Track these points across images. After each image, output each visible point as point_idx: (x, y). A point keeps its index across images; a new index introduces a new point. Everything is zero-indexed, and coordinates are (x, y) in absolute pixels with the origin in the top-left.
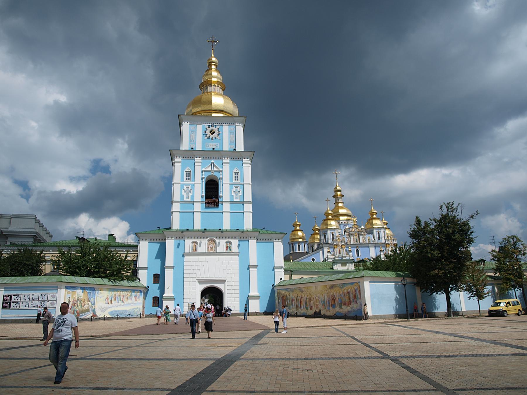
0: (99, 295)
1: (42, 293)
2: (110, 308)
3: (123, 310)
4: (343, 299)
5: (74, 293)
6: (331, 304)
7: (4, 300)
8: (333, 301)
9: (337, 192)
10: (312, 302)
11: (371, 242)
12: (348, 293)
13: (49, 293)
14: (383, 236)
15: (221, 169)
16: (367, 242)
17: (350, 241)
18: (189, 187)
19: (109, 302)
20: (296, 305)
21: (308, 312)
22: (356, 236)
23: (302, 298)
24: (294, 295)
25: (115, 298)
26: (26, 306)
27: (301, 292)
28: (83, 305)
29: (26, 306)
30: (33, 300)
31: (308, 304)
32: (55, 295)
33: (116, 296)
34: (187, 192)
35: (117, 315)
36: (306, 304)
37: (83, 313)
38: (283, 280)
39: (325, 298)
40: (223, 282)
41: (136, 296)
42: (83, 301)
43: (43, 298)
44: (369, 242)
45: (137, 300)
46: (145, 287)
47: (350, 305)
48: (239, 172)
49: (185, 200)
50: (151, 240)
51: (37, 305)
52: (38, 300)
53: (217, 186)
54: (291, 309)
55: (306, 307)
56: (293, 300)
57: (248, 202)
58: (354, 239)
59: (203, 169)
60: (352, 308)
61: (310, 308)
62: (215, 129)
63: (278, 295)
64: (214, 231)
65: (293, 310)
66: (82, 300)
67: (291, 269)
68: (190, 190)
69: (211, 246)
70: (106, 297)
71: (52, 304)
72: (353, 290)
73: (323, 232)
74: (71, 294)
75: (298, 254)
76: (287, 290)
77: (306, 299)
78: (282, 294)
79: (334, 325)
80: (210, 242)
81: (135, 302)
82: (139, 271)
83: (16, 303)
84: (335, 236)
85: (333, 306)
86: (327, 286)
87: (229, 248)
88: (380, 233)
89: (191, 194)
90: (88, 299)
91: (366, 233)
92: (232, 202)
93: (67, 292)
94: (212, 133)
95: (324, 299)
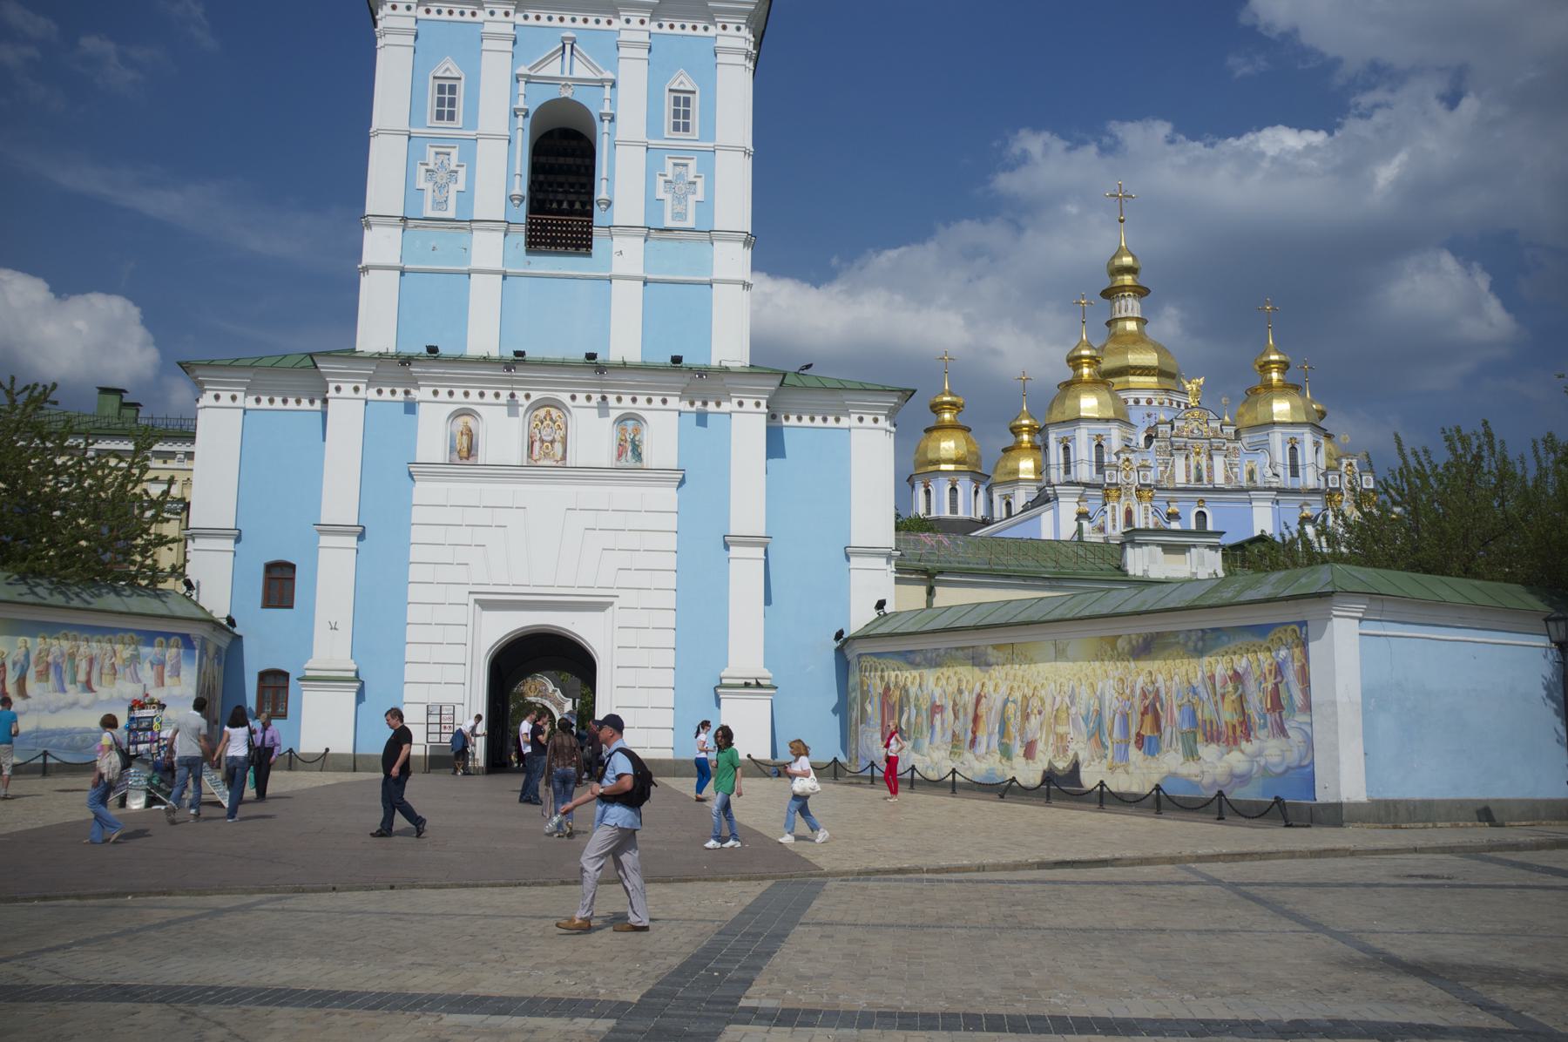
4: (1205, 712)
6: (1138, 734)
8: (1149, 718)
9: (1122, 274)
10: (1034, 721)
11: (1260, 483)
12: (1237, 677)
15: (608, 75)
16: (1245, 484)
17: (1172, 476)
18: (448, 154)
21: (1012, 768)
22: (1198, 454)
23: (983, 700)
24: (945, 683)
25: (40, 668)
31: (1013, 730)
33: (50, 659)
34: (441, 177)
35: (45, 754)
36: (1003, 730)
38: (888, 609)
39: (1107, 703)
41: (162, 664)
44: (1253, 485)
45: (167, 680)
46: (214, 624)
47: (1244, 744)
48: (694, 92)
49: (425, 215)
53: (587, 161)
54: (926, 750)
55: (1001, 744)
56: (935, 709)
57: (729, 235)
58: (1188, 467)
59: (523, 70)
60: (1252, 758)
64: (563, 365)
67: (929, 566)
68: (453, 167)
72: (1266, 667)
76: (912, 656)
79: (1200, 859)
80: (542, 413)
84: (1110, 448)
86: (1120, 641)
87: (631, 448)
88: (1297, 446)
89: (461, 186)
91: (1239, 445)
92: (655, 231)
95: (1101, 700)
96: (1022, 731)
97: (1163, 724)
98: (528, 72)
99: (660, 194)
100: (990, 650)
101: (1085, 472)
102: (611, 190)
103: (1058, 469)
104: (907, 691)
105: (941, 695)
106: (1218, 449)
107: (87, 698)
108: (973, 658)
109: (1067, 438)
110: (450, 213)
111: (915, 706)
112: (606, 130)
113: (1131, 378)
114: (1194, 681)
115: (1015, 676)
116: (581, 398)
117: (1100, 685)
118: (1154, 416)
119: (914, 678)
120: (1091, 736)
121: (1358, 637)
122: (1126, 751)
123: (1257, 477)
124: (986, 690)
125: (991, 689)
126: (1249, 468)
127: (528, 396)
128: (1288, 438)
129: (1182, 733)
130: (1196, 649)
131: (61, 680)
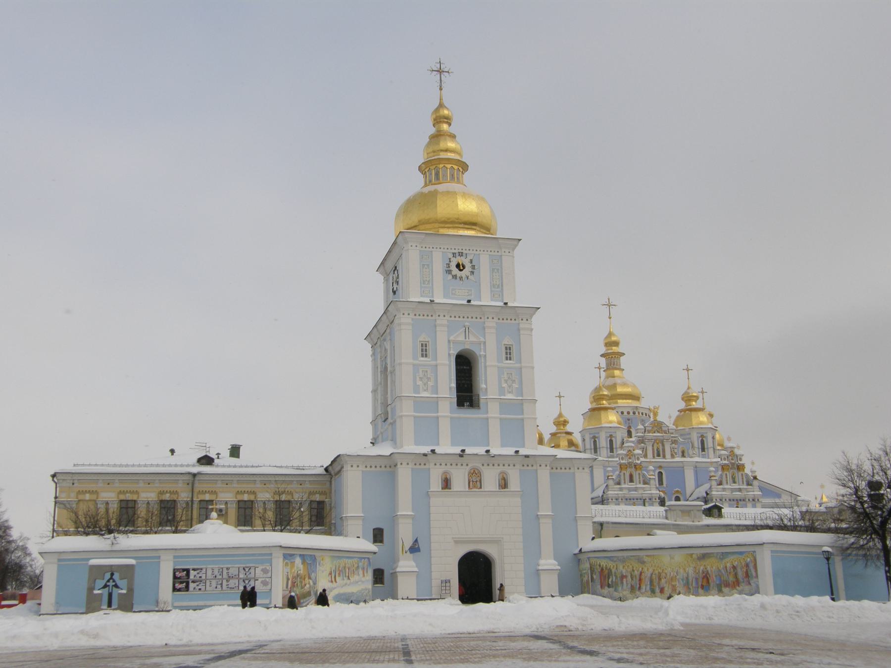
0: (321, 568)
1: (244, 566)
2: (334, 588)
3: (349, 593)
5: (293, 563)
6: (702, 585)
7: (175, 577)
8: (705, 580)
10: (663, 581)
13: (257, 566)
14: (712, 446)
15: (482, 339)
19: (333, 580)
20: (629, 586)
22: (658, 444)
23: (643, 574)
26: (216, 587)
27: (641, 563)
28: (303, 584)
29: (216, 587)
30: (230, 578)
31: (655, 584)
32: (268, 568)
37: (304, 598)
39: (690, 575)
40: (497, 542)
41: (364, 569)
42: (303, 577)
43: (247, 574)
45: (365, 574)
47: (737, 587)
48: (512, 345)
50: (366, 467)
51: (237, 585)
52: (237, 576)
55: (651, 589)
56: (623, 577)
58: (653, 449)
59: (452, 338)
61: (659, 591)
63: (591, 567)
66: (301, 577)
68: (429, 376)
70: (328, 572)
71: (265, 583)
72: (743, 564)
74: (289, 567)
77: (652, 574)
78: (600, 566)
81: (363, 579)
82: (350, 522)
83: (198, 583)
87: (504, 484)
88: (704, 439)
89: (431, 384)
90: (309, 574)
93: (285, 563)
95: (688, 575)
96: (659, 583)
97: (710, 581)
98: (454, 339)
99: (504, 385)
100: (644, 557)
102: (486, 384)
104: (611, 570)
105: (625, 573)
107: (348, 582)
108: (638, 559)
109: (595, 436)
111: (615, 576)
112: (483, 361)
113: (619, 401)
114: (720, 568)
115: (655, 566)
116: (485, 465)
117: (687, 569)
118: (631, 420)
119: (614, 566)
120: (684, 585)
121: (770, 556)
122: (698, 590)
124: (644, 570)
125: (646, 570)
126: (682, 450)
127: (467, 465)
128: (700, 435)
129: (717, 585)
130: (720, 558)
131: (343, 575)
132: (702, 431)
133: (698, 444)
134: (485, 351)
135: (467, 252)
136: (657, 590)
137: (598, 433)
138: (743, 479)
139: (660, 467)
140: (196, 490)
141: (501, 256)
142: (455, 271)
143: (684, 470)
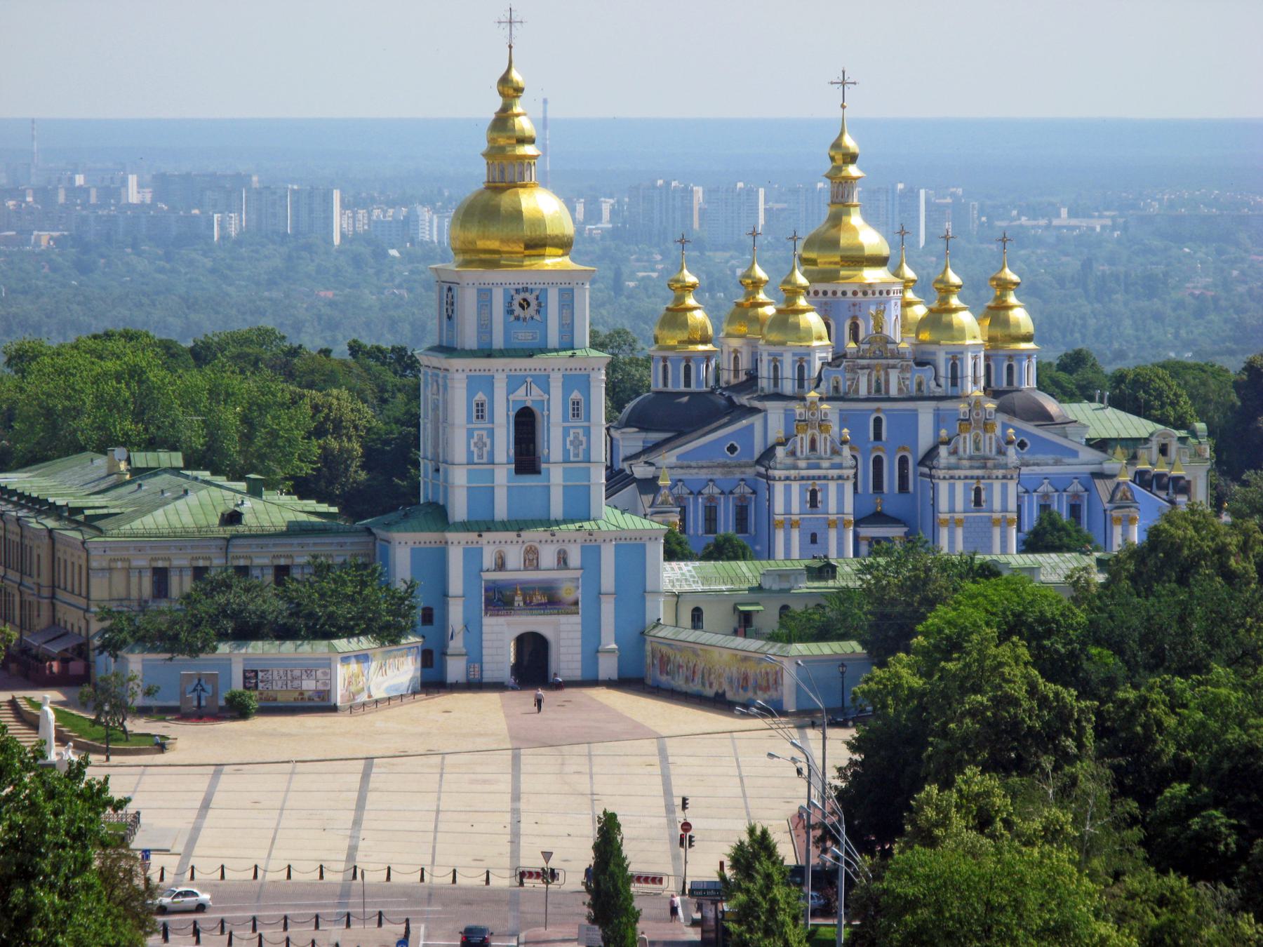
4: (759, 681)
7: (245, 678)
10: (713, 676)
11: (926, 393)
12: (767, 673)
17: (857, 391)
22: (878, 371)
30: (294, 679)
34: (480, 444)
36: (703, 676)
44: (920, 394)
56: (680, 666)
58: (869, 381)
62: (531, 298)
65: (679, 683)
69: (531, 556)
73: (769, 355)
75: (685, 399)
85: (745, 688)
87: (563, 560)
94: (525, 304)
101: (788, 387)
103: (769, 383)
106: (894, 367)
110: (485, 460)
123: (924, 388)
128: (950, 356)
132: (953, 349)
133: (947, 370)
134: (549, 410)
135: (533, 286)
136: (707, 685)
137: (781, 355)
138: (990, 444)
139: (878, 410)
140: (230, 555)
141: (572, 290)
142: (518, 311)
143: (917, 415)
